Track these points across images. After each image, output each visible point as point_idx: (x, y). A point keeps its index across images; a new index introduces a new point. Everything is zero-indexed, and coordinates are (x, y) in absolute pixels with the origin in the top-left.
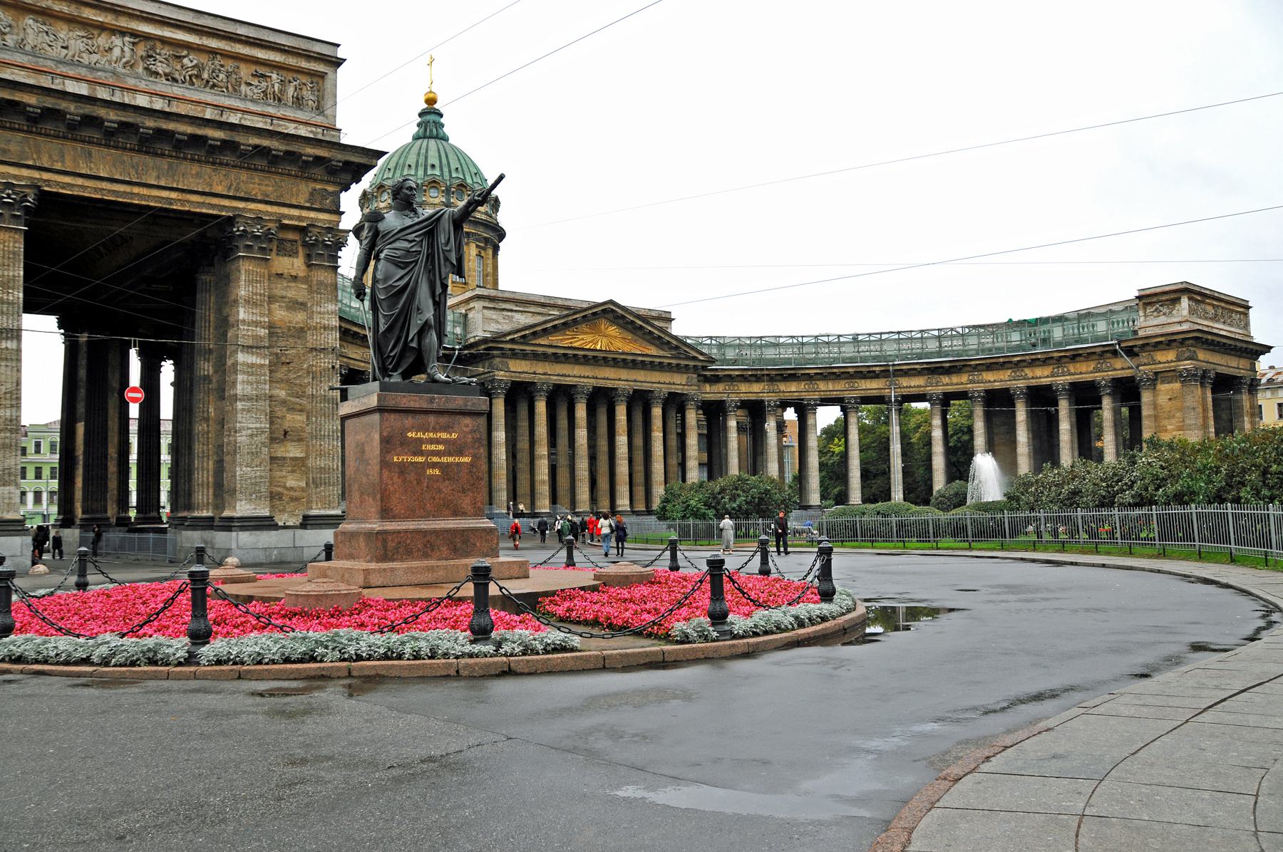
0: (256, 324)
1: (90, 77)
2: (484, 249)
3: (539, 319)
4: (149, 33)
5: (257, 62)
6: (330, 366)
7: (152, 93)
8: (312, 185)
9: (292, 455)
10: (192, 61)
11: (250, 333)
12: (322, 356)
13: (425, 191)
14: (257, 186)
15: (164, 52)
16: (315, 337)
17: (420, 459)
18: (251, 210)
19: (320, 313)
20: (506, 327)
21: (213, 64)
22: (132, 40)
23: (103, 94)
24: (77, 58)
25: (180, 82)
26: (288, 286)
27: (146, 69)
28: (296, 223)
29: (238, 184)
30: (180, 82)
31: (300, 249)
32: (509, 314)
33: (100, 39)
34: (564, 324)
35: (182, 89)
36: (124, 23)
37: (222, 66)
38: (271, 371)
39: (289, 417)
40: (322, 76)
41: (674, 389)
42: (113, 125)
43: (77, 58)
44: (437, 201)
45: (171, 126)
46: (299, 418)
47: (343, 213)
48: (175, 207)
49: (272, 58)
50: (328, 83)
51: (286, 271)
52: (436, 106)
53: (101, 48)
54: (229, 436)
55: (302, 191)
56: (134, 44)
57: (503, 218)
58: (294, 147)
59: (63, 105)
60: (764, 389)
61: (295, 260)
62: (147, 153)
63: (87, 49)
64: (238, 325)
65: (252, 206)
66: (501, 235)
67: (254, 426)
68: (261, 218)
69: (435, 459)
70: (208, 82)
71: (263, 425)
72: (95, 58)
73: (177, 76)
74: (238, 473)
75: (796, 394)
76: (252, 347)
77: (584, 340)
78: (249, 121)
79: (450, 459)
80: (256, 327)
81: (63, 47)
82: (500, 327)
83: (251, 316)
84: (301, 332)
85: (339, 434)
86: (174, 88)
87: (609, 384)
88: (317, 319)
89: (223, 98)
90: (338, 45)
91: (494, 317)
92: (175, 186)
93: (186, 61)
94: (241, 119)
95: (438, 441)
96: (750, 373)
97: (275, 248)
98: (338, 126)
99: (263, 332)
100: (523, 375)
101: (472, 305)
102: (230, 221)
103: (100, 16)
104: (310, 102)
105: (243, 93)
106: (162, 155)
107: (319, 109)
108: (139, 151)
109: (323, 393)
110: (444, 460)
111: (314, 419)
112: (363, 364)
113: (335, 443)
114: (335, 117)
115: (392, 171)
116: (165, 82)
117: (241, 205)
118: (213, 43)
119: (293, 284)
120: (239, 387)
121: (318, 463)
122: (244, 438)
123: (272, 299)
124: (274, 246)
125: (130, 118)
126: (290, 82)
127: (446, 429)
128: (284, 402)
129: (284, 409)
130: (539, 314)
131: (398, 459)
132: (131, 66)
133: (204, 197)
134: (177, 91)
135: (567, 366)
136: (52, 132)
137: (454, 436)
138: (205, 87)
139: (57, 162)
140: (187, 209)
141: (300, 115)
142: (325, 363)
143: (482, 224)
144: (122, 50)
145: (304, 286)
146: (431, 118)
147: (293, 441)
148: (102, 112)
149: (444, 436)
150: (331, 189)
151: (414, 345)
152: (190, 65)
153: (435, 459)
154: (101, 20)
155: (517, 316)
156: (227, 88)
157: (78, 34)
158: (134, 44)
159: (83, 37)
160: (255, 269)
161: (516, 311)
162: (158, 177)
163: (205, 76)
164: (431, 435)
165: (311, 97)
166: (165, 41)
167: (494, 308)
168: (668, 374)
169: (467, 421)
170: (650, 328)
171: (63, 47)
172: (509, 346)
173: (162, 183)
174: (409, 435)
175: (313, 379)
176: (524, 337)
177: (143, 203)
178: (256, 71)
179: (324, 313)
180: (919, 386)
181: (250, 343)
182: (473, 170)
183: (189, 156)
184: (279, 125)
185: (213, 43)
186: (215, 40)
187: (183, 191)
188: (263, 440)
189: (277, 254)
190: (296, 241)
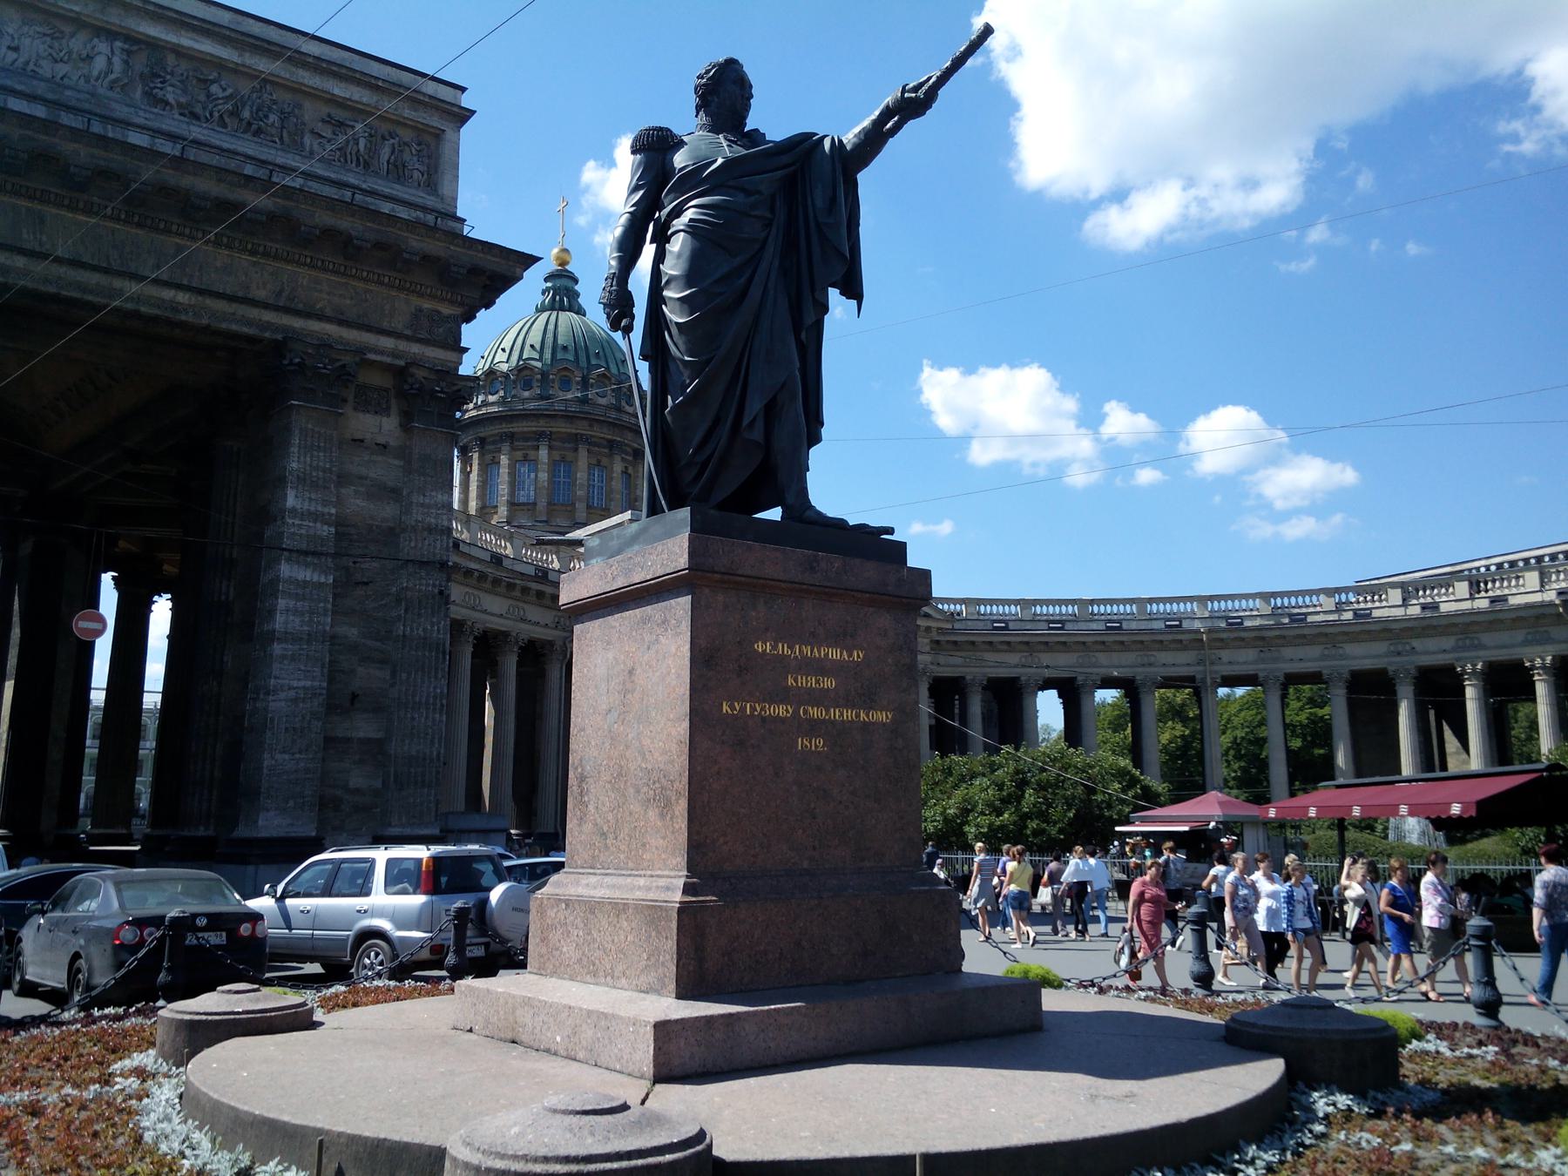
0: (316, 517)
1: (50, 96)
4: (154, 38)
5: (334, 101)
6: (436, 591)
7: (154, 131)
8: (416, 301)
9: (361, 735)
10: (224, 90)
11: (303, 532)
13: (553, 381)
14: (325, 296)
16: (413, 544)
17: (782, 711)
19: (422, 505)
22: (126, 46)
24: (31, 64)
25: (203, 119)
27: (148, 94)
28: (388, 360)
30: (203, 119)
31: (393, 401)
33: (73, 40)
35: (205, 132)
37: (275, 102)
38: (335, 596)
39: (360, 670)
40: (438, 135)
43: (31, 66)
44: (569, 396)
45: (187, 181)
47: (466, 350)
48: (183, 318)
49: (356, 97)
50: (446, 149)
51: (368, 436)
53: (74, 56)
54: (255, 700)
55: (401, 307)
61: (385, 419)
62: (139, 225)
63: (50, 54)
64: (283, 517)
65: (315, 326)
67: (302, 683)
68: (331, 347)
69: (815, 712)
70: (249, 124)
71: (316, 684)
72: (62, 69)
73: (198, 109)
74: (266, 763)
76: (306, 553)
79: (848, 715)
80: (315, 521)
81: (9, 48)
83: (306, 503)
84: (391, 534)
85: (444, 702)
86: (192, 128)
89: (273, 151)
92: (185, 282)
93: (214, 88)
95: (820, 668)
97: (351, 398)
99: (326, 531)
102: (279, 347)
104: (416, 174)
106: (167, 231)
108: (126, 222)
110: (835, 714)
111: (404, 676)
114: (455, 199)
115: (508, 351)
117: (297, 323)
118: (263, 65)
119: (380, 458)
121: (406, 748)
122: (283, 704)
123: (343, 479)
126: (384, 138)
127: (840, 638)
131: (732, 708)
133: (234, 305)
134: (197, 132)
137: (857, 655)
138: (245, 132)
140: (205, 321)
142: (428, 585)
143: (627, 427)
144: (109, 60)
145: (396, 462)
146: (559, 282)
148: (67, 147)
149: (834, 654)
150: (446, 310)
152: (221, 96)
153: (815, 712)
154: (76, 8)
156: (281, 138)
157: (38, 29)
158: (129, 53)
159: (45, 35)
160: (316, 429)
163: (246, 114)
164: (807, 650)
165: (417, 166)
166: (178, 51)
169: (884, 620)
171: (9, 48)
175: (406, 611)
178: (329, 116)
181: (304, 546)
185: (263, 65)
186: (264, 60)
187: (200, 292)
189: (355, 409)
190: (386, 390)
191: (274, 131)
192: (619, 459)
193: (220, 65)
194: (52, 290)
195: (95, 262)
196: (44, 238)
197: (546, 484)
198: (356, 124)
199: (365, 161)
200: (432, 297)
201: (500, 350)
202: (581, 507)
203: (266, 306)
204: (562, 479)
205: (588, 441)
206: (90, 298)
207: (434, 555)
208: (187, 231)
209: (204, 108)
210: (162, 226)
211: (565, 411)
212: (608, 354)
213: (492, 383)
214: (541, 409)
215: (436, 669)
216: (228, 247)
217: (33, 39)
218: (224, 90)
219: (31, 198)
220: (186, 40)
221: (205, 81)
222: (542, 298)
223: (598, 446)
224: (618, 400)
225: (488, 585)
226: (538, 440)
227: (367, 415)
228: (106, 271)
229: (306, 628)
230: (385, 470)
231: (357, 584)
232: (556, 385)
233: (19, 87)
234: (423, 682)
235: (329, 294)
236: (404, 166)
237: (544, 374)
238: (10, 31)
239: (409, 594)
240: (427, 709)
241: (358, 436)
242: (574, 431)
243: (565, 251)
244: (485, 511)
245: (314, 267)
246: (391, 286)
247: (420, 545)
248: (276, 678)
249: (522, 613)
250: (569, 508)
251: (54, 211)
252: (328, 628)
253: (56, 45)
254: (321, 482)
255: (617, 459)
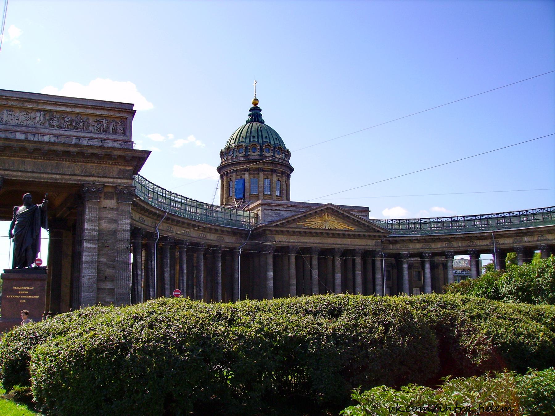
1: (26, 130)
2: (282, 177)
3: (294, 213)
5: (97, 115)
8: (119, 167)
9: (108, 287)
10: (68, 119)
12: (122, 243)
13: (250, 149)
15: (57, 116)
16: (119, 235)
17: (18, 297)
18: (91, 181)
19: (122, 224)
20: (277, 219)
21: (77, 119)
22: (44, 113)
23: (31, 138)
24: (22, 123)
26: (109, 213)
27: (49, 124)
28: (112, 185)
29: (86, 169)
31: (115, 195)
32: (278, 212)
34: (305, 216)
35: (63, 131)
36: (41, 107)
37: (81, 119)
38: (99, 251)
39: (107, 270)
40: (126, 118)
41: (367, 248)
42: (31, 150)
43: (22, 123)
44: (255, 154)
45: (55, 148)
46: (112, 271)
48: (58, 182)
50: (128, 122)
51: (108, 206)
52: (257, 106)
56: (45, 115)
57: (292, 161)
58: (109, 151)
59: (12, 143)
60: (423, 246)
61: (112, 201)
62: (47, 160)
65: (92, 179)
66: (292, 170)
67: (90, 275)
69: (24, 297)
70: (75, 126)
71: (94, 274)
72: (29, 122)
73: (62, 126)
75: (441, 249)
76: (90, 240)
77: (315, 223)
78: (91, 143)
79: (30, 297)
81: (17, 120)
82: (273, 219)
87: (330, 246)
88: (120, 227)
89: (81, 133)
90: (133, 105)
91: (270, 214)
92: (59, 172)
93: (66, 119)
94: (88, 141)
96: (414, 238)
98: (132, 140)
100: (282, 243)
101: (259, 209)
102: (83, 185)
103: (31, 105)
104: (120, 131)
105: (90, 130)
106: (54, 160)
107: (124, 133)
108: (44, 159)
109: (122, 260)
110: (27, 297)
111: (118, 271)
112: (199, 240)
113: (127, 282)
116: (56, 129)
117: (87, 179)
118: (78, 110)
119: (111, 212)
120: (84, 258)
121: (119, 291)
122: (86, 280)
123: (100, 219)
124: (102, 195)
125: (39, 146)
126: (111, 123)
128: (105, 264)
129: (106, 267)
130: (294, 211)
132: (43, 124)
133: (71, 176)
134: (62, 132)
135: (306, 237)
136: (9, 155)
139: (11, 166)
140: (64, 182)
141: (115, 137)
142: (123, 246)
145: (116, 212)
146: (254, 112)
147: (109, 281)
148: (27, 145)
149: (28, 288)
150: (128, 168)
151: (24, 255)
153: (24, 297)
154: (31, 106)
155: (282, 213)
156: (83, 129)
158: (45, 115)
159: (25, 114)
161: (282, 210)
162: (52, 170)
163: (74, 124)
164: (23, 288)
166: (57, 112)
167: (270, 209)
168: (364, 240)
169: (39, 283)
170: (352, 217)
171: (17, 120)
172: (274, 229)
173: (53, 171)
174: (14, 288)
175: (118, 254)
176: (282, 223)
177: (45, 181)
179: (124, 224)
180: (510, 244)
181: (90, 238)
182: (275, 137)
183: (65, 160)
184: (105, 143)
185: (78, 110)
187: (62, 174)
188: (94, 281)
189: (104, 199)
191: (81, 127)
192: (275, 175)
193: (67, 112)
194: (27, 179)
195: (37, 171)
196: (25, 167)
197: (248, 187)
198: (103, 121)
199: (106, 130)
200: (123, 165)
201: (232, 140)
202: (261, 194)
203: (79, 175)
204: (254, 185)
205: (263, 170)
206: (36, 180)
207: (125, 237)
208: (58, 159)
209: (64, 124)
210: (52, 159)
211: (254, 160)
212: (270, 137)
213: (229, 151)
214: (244, 160)
215: (127, 269)
216: (69, 161)
217: (22, 116)
218: (68, 119)
219: (21, 157)
220: (58, 108)
221: (64, 117)
222: (249, 117)
223: (268, 171)
224: (274, 153)
225: (208, 230)
226: (245, 171)
227: (108, 200)
228: (39, 173)
229: (91, 260)
230: (111, 215)
231: (106, 247)
232: (251, 151)
233: (19, 130)
234: (123, 273)
235: (95, 169)
236: (117, 129)
237: (246, 147)
238: (17, 115)
239: (118, 249)
240: (124, 280)
241: (105, 206)
242: (257, 167)
243: (256, 100)
244: (229, 198)
245: (90, 163)
246: (112, 164)
247: (121, 235)
248: (84, 273)
249: (222, 239)
250: (257, 196)
251: (27, 159)
252: (97, 260)
253: (27, 116)
254: (94, 220)
255: (274, 176)
